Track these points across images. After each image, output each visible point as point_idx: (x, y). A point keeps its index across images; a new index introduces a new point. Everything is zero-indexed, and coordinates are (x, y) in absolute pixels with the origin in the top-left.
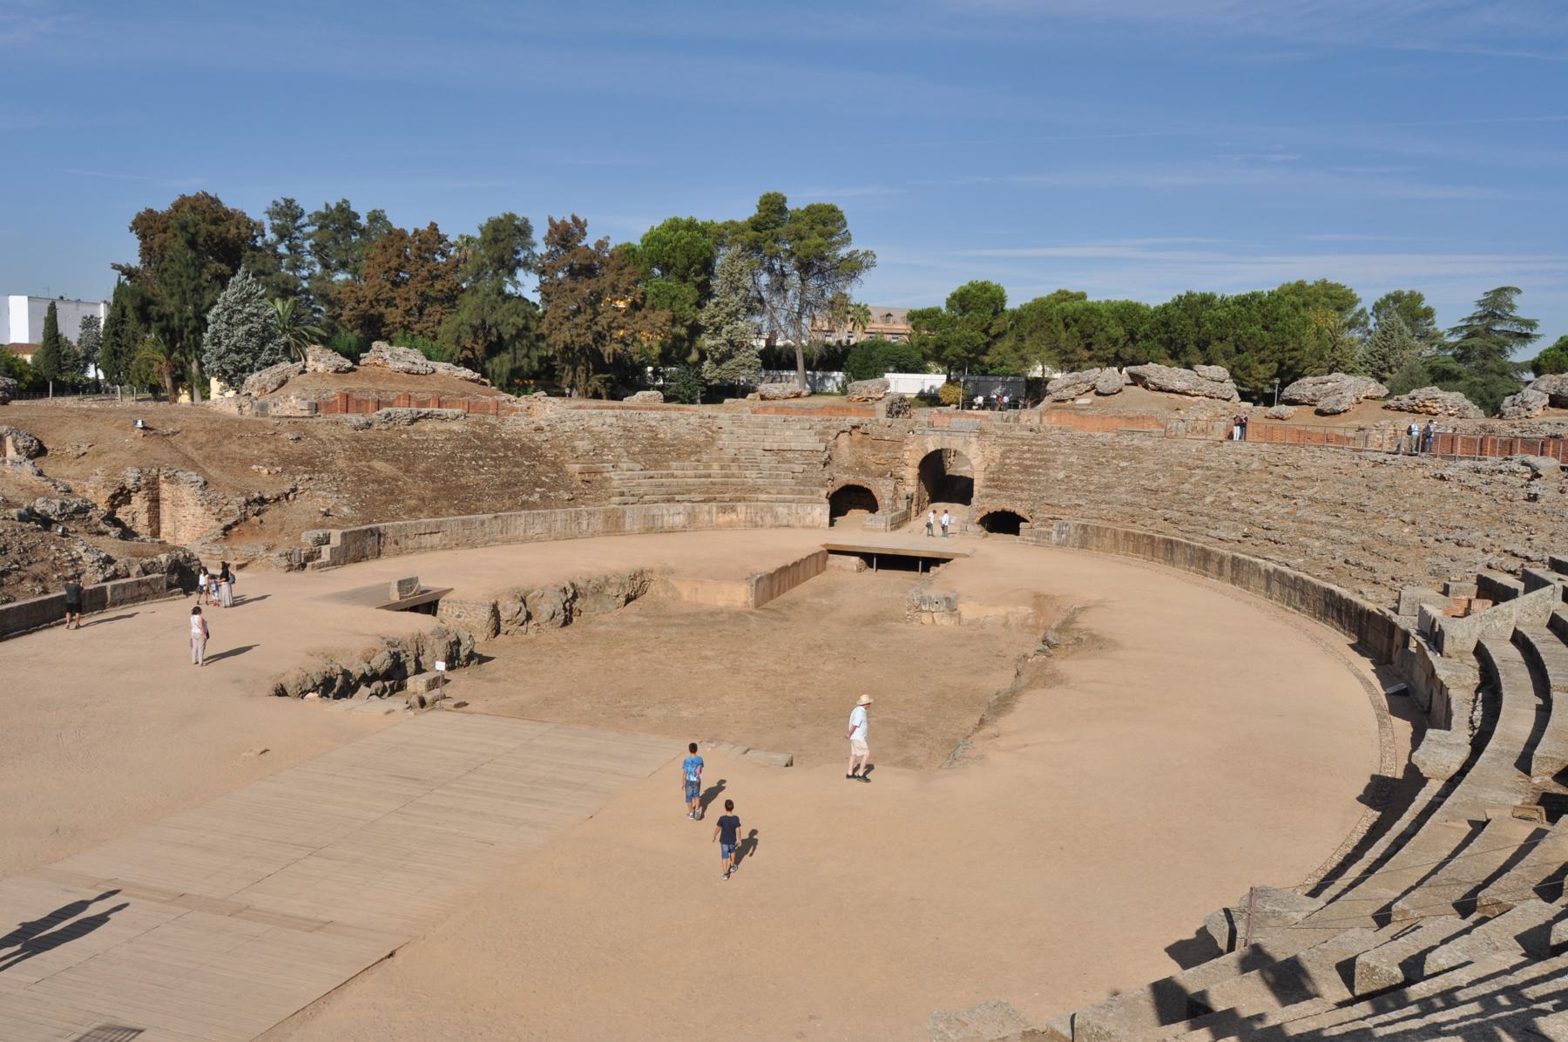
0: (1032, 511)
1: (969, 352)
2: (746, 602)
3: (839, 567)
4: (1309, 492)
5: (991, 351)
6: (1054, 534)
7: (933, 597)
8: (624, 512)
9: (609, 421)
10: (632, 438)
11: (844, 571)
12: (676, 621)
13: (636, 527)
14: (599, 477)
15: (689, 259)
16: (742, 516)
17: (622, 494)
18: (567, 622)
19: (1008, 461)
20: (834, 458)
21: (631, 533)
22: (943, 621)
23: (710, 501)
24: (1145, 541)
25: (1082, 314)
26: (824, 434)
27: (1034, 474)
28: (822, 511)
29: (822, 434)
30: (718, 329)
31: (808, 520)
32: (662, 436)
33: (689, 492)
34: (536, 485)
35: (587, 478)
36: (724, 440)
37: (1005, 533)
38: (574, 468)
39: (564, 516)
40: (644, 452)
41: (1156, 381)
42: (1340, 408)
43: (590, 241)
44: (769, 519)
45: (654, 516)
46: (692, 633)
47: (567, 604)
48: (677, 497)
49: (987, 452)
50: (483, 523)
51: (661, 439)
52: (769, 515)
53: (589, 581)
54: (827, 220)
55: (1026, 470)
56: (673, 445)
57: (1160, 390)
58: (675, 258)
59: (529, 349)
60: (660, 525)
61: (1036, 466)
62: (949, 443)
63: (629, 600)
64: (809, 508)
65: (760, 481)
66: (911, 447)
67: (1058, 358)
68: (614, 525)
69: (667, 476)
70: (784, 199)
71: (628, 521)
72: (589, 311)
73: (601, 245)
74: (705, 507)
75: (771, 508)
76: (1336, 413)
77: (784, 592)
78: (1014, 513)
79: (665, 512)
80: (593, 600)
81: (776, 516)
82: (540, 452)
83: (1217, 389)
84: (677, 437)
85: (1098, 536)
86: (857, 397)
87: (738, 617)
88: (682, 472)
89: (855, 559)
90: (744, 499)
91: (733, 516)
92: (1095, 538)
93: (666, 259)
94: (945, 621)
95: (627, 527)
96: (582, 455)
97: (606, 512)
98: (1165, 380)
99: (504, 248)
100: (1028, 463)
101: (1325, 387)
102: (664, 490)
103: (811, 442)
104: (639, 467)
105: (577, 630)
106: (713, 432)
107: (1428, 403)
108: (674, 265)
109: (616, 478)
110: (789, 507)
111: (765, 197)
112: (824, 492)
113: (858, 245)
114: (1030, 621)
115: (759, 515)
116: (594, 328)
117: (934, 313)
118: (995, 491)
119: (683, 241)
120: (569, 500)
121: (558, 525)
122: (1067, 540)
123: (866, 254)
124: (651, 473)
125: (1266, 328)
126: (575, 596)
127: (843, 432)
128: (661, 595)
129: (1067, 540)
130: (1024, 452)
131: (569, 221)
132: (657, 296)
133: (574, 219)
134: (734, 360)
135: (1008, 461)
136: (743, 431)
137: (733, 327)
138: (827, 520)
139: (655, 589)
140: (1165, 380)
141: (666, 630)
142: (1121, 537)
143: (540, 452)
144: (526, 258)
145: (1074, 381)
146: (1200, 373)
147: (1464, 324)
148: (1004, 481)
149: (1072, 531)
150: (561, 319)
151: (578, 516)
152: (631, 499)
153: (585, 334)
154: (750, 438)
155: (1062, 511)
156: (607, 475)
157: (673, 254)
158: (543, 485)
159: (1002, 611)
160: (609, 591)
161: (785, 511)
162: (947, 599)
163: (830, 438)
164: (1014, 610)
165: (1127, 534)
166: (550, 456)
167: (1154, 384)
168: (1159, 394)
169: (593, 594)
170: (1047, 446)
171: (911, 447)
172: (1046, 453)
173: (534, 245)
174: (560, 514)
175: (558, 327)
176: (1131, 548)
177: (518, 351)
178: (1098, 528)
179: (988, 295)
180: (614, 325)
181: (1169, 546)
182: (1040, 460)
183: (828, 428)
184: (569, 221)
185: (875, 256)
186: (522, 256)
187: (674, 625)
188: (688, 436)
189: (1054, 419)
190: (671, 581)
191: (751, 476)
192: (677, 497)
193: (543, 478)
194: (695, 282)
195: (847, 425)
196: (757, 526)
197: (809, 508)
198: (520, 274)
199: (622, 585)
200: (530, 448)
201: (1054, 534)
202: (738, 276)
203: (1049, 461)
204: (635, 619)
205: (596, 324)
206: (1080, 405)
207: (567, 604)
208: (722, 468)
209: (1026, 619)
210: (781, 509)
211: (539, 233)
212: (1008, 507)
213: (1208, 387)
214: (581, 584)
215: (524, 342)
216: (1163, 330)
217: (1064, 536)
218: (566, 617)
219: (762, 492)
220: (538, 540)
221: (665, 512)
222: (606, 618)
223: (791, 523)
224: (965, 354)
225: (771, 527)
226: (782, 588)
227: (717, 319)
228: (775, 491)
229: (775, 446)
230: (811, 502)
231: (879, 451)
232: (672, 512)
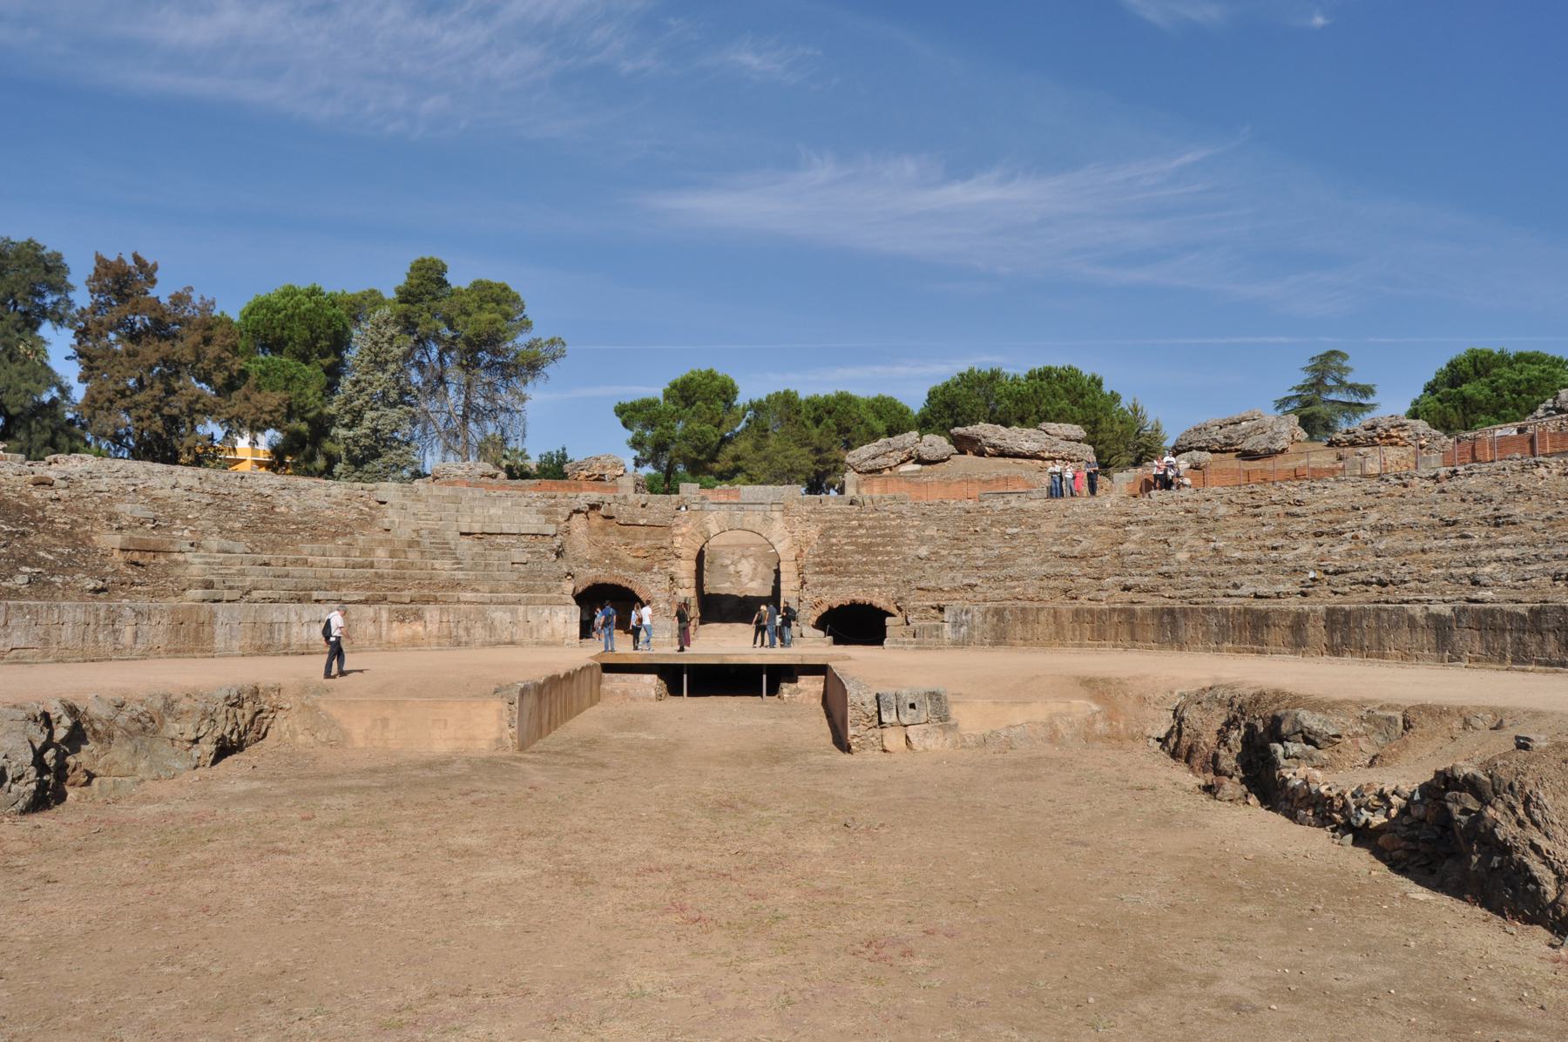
0: (901, 599)
1: (700, 453)
2: (499, 740)
3: (625, 693)
4: (1373, 517)
5: (721, 457)
6: (947, 627)
7: (904, 692)
8: (213, 615)
9: (184, 482)
10: (229, 509)
11: (633, 699)
12: (348, 783)
13: (235, 644)
14: (162, 559)
15: (312, 332)
16: (433, 628)
17: (209, 585)
18: (46, 798)
19: (834, 540)
20: (568, 550)
21: (227, 654)
22: (929, 742)
23: (376, 602)
24: (1116, 619)
25: (837, 404)
26: (550, 513)
27: (881, 553)
28: (568, 618)
29: (549, 513)
30: (357, 417)
31: (545, 632)
32: (283, 509)
33: (337, 586)
34: (23, 561)
35: (136, 556)
36: (391, 516)
37: (846, 644)
38: (108, 540)
39: (80, 616)
40: (249, 527)
41: (993, 441)
42: (1278, 446)
43: (162, 292)
44: (479, 632)
45: (271, 624)
46: (398, 803)
47: (49, 755)
48: (315, 595)
49: (798, 533)
51: (282, 514)
52: (479, 624)
53: (120, 706)
54: (498, 298)
55: (867, 549)
56: (305, 523)
57: (1003, 454)
58: (291, 329)
59: (54, 433)
60: (284, 640)
61: (879, 545)
62: (742, 520)
63: (224, 750)
64: (547, 612)
65: (460, 575)
66: (684, 530)
67: (812, 457)
69: (295, 562)
70: (444, 268)
71: (220, 631)
72: (158, 385)
73: (179, 300)
74: (369, 611)
75: (483, 613)
76: (1270, 454)
77: (556, 728)
78: (870, 605)
79: (293, 618)
80: (129, 747)
81: (491, 627)
82: (40, 514)
84: (312, 511)
85: (1024, 622)
86: (585, 473)
87: (490, 766)
88: (326, 559)
89: (651, 680)
90: (436, 600)
91: (418, 627)
92: (1020, 627)
93: (278, 330)
94: (930, 741)
95: (219, 643)
96: (130, 527)
97: (174, 611)
98: (1008, 441)
99: (16, 282)
100: (865, 540)
101: (1239, 428)
102: (290, 583)
103: (533, 522)
104: (239, 547)
105: (73, 819)
106: (370, 508)
107: (1393, 432)
108: (290, 338)
109: (197, 560)
110: (513, 612)
111: (418, 262)
112: (569, 586)
113: (541, 331)
114: (1101, 727)
115: (462, 625)
116: (166, 410)
117: (650, 404)
118: (833, 578)
119: (303, 308)
120: (97, 591)
121: (67, 632)
122: (970, 636)
123: (552, 342)
124: (266, 557)
125: (1075, 403)
126: (77, 737)
127: (578, 512)
128: (301, 738)
129: (970, 636)
130: (854, 528)
131: (130, 262)
132: (266, 375)
133: (137, 258)
134: (381, 460)
135: (834, 540)
136: (421, 506)
137: (380, 413)
138: (576, 630)
139: (281, 727)
140: (1008, 441)
141: (333, 801)
142: (1066, 619)
143: (40, 514)
144: (56, 304)
145: (883, 450)
146: (1051, 431)
147: (1294, 393)
148: (840, 565)
149: (978, 619)
150: (111, 395)
151: (113, 618)
152: (227, 594)
153: (149, 418)
154: (435, 515)
155: (947, 596)
156: (180, 558)
157: (289, 324)
158: (39, 562)
159: (1039, 712)
160: (173, 728)
161: (507, 617)
162: (934, 696)
163: (561, 519)
164: (1062, 707)
165: (1077, 614)
166: (61, 521)
167: (994, 446)
168: (1001, 460)
169: (130, 735)
170: (885, 519)
171: (684, 530)
172: (886, 527)
173: (70, 288)
174: (73, 612)
175: (107, 404)
176: (1088, 634)
177: (36, 437)
178: (1023, 610)
179: (717, 383)
180: (199, 406)
181: (1166, 619)
182: (883, 536)
183: (555, 505)
184: (130, 262)
185: (564, 344)
186: (50, 299)
187: (349, 789)
188: (328, 512)
189: (876, 489)
190: (323, 706)
191: (444, 568)
193: (42, 554)
194: (322, 365)
195: (581, 503)
196: (459, 644)
197: (547, 612)
198: (46, 330)
199: (209, 716)
200: (19, 508)
201: (947, 627)
202: (386, 345)
203: (896, 537)
204: (241, 787)
205: (168, 404)
206: (906, 472)
207: (49, 755)
208: (393, 554)
209: (1090, 722)
210: (500, 615)
211: (79, 273)
212: (861, 597)
213: (1064, 448)
214: (97, 710)
215: (47, 422)
216: (946, 414)
217: (964, 629)
218: (42, 786)
219: (464, 588)
220: (18, 661)
221: (293, 618)
222: (162, 789)
223: (516, 638)
224: (694, 455)
225: (483, 646)
226: (553, 720)
227: (356, 403)
228: (487, 588)
229: (477, 528)
230: (548, 603)
231: (635, 539)
232: (306, 618)
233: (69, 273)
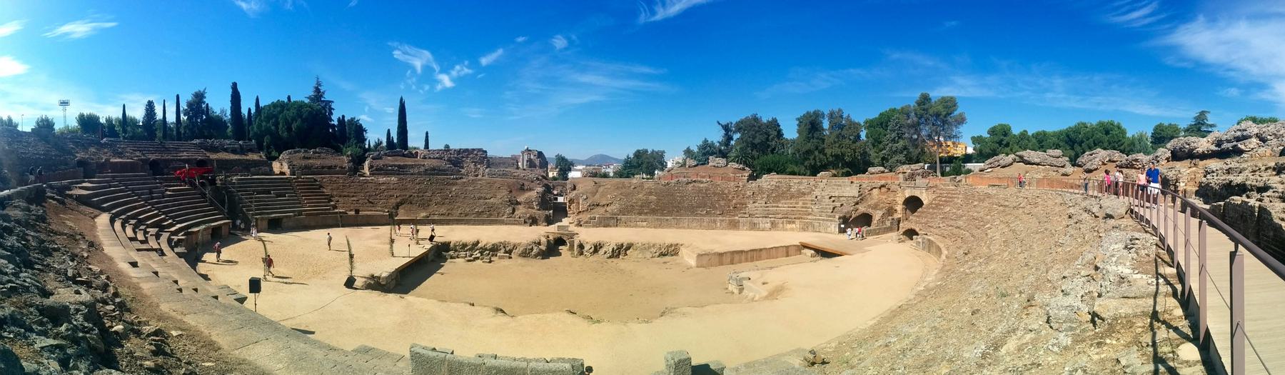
28: (834, 227)
48: (770, 216)
50: (667, 220)
68: (734, 225)
74: (781, 221)
83: (1054, 161)
91: (794, 225)
127: (875, 188)
151: (715, 222)
189: (971, 180)
192: (770, 216)
208: (803, 204)
230: (831, 221)
233: (819, 111)
